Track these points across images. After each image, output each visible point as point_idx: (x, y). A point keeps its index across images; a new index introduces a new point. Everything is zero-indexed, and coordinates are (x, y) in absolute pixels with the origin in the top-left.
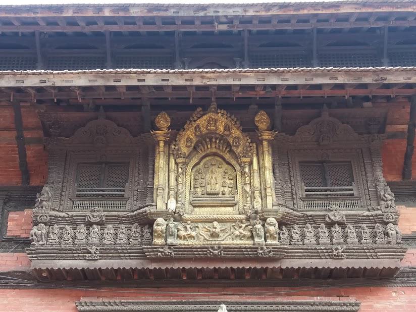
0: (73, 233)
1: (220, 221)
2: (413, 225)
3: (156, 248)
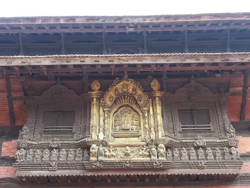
0: (41, 154)
1: (130, 146)
2: (247, 148)
3: (91, 163)
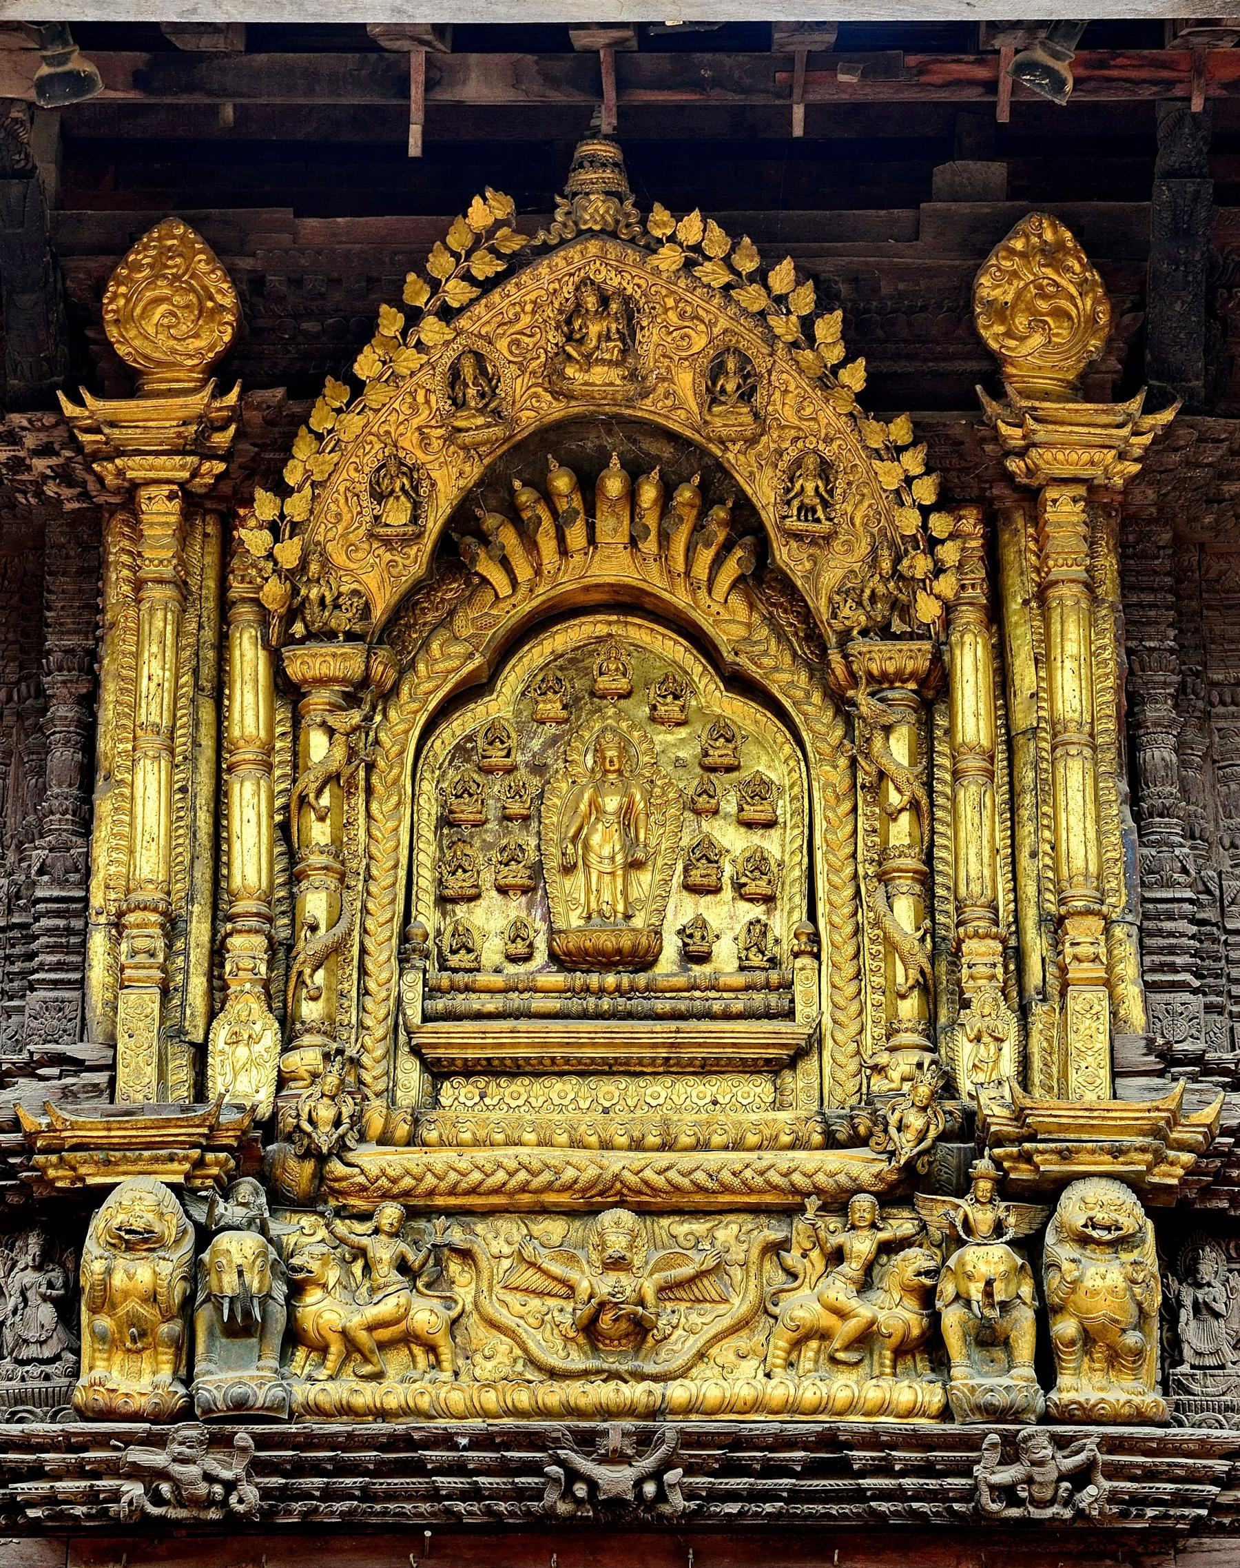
3: (101, 1441)
